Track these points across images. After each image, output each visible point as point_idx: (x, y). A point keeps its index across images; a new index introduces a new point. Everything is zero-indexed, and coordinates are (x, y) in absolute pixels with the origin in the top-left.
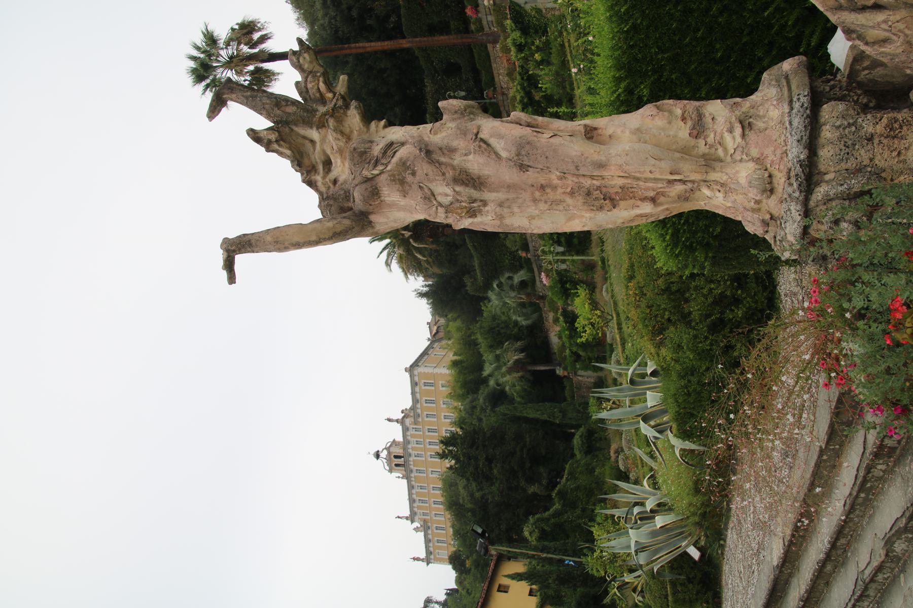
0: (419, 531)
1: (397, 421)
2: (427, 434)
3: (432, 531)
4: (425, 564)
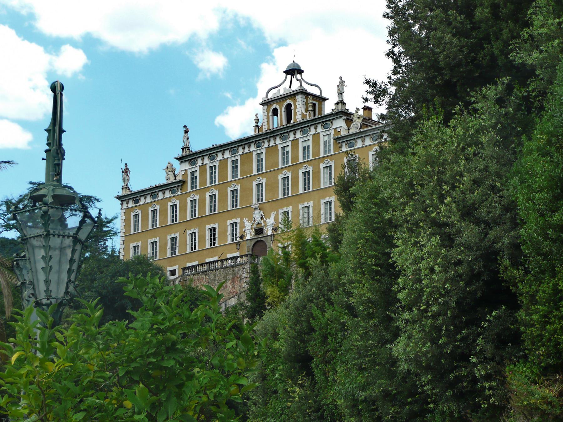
1: (341, 103)
2: (301, 172)
3: (169, 199)
4: (121, 193)
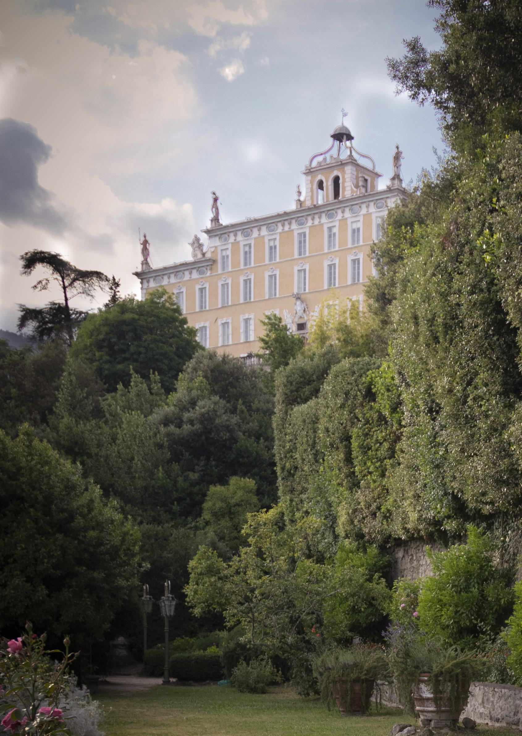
0: (194, 250)
4: (139, 270)
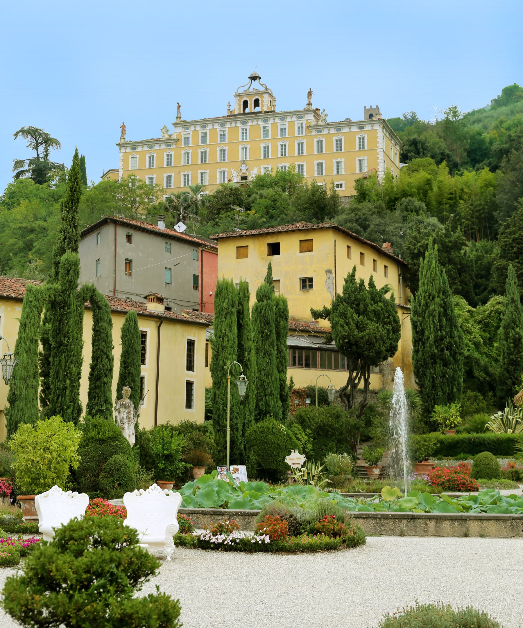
1: (309, 104)
4: (118, 141)
